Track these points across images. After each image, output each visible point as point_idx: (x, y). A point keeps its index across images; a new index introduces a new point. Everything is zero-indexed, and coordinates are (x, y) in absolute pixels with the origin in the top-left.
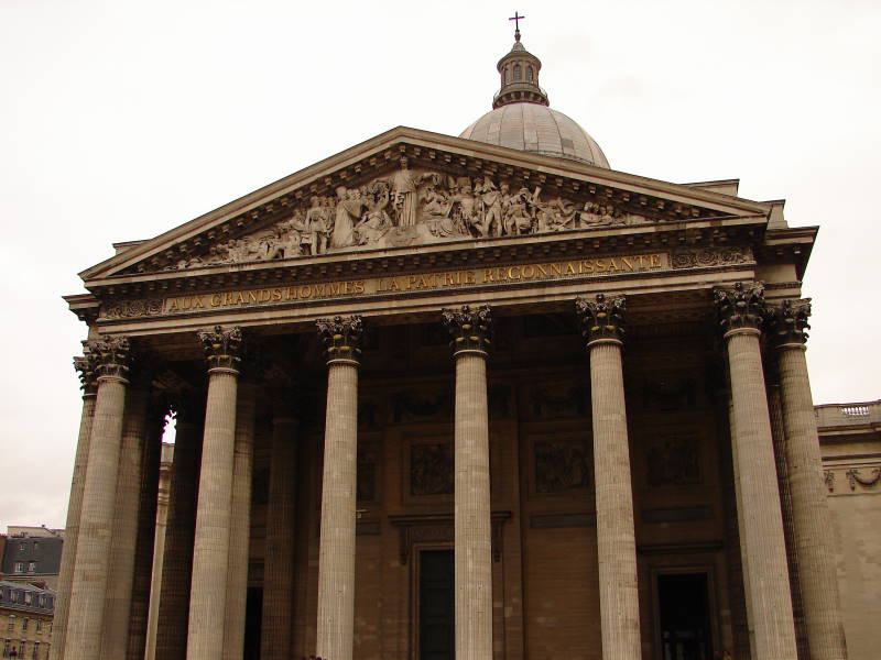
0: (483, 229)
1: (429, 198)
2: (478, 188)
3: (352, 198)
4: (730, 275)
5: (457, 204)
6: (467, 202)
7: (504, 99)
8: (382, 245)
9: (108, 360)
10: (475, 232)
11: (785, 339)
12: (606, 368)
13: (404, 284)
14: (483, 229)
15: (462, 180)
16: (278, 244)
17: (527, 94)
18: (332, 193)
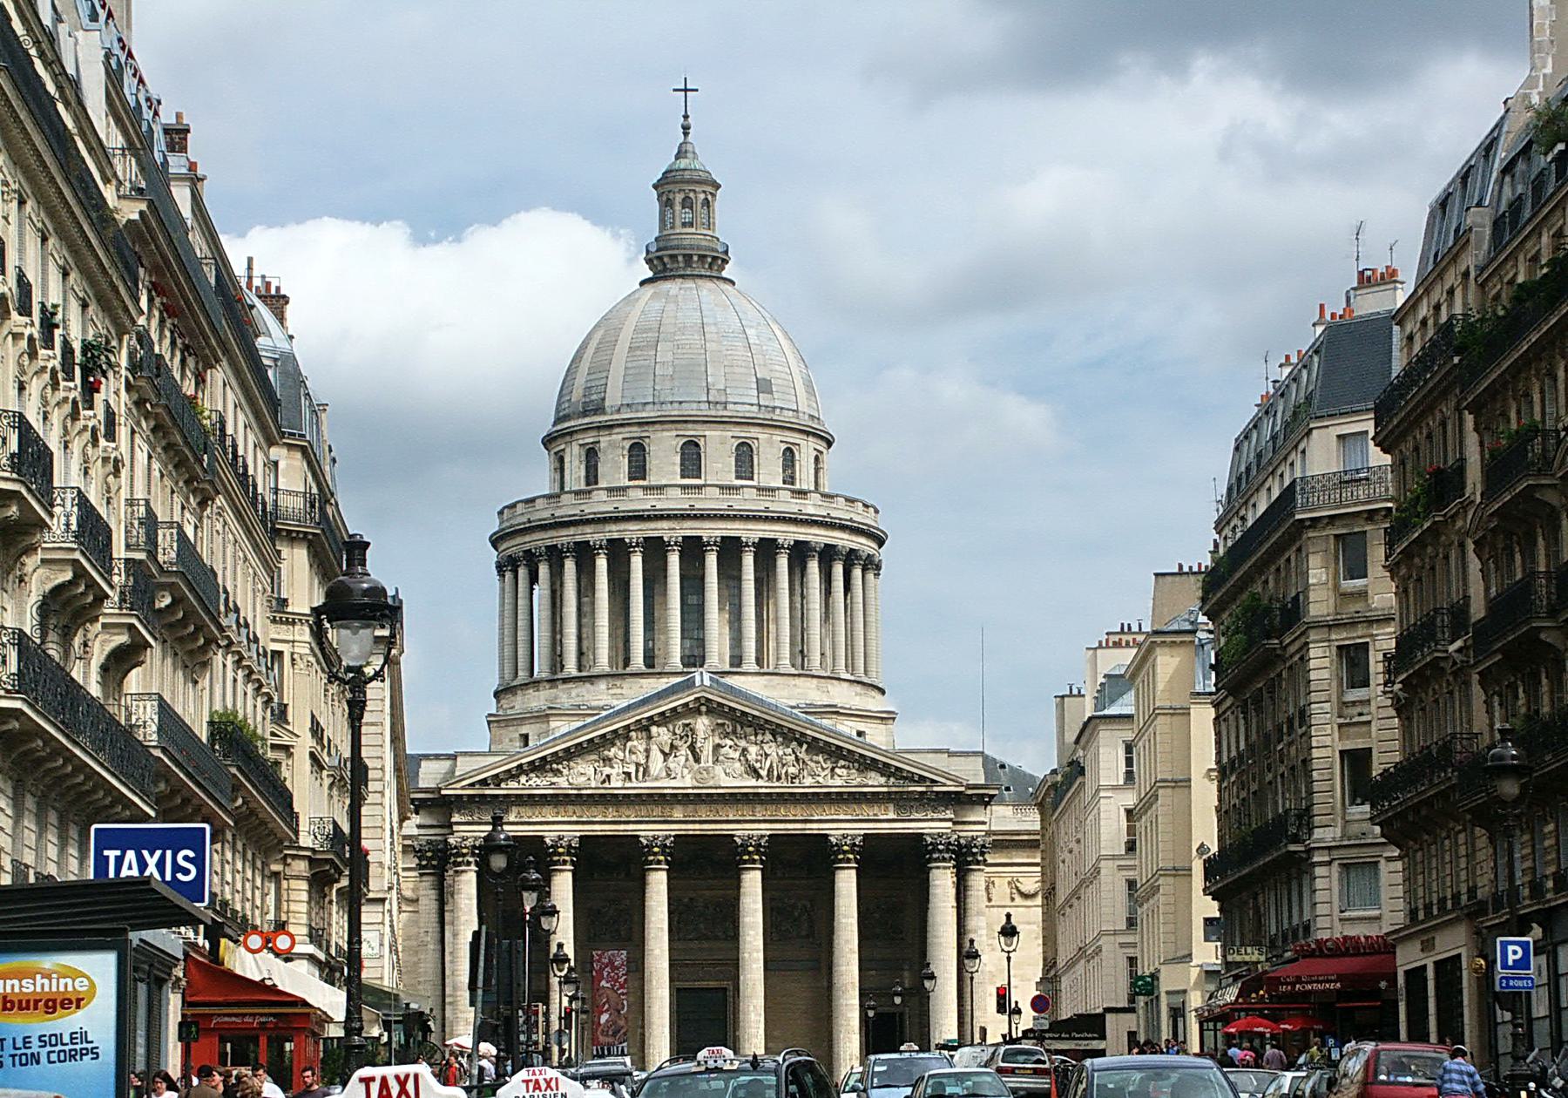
0: (764, 773)
1: (722, 742)
2: (760, 738)
3: (662, 734)
4: (933, 825)
5: (745, 750)
6: (753, 749)
7: (666, 260)
8: (688, 782)
9: (464, 855)
10: (759, 776)
11: (970, 863)
12: (847, 883)
13: (704, 812)
14: (764, 773)
15: (749, 730)
16: (607, 770)
17: (702, 257)
18: (647, 729)
